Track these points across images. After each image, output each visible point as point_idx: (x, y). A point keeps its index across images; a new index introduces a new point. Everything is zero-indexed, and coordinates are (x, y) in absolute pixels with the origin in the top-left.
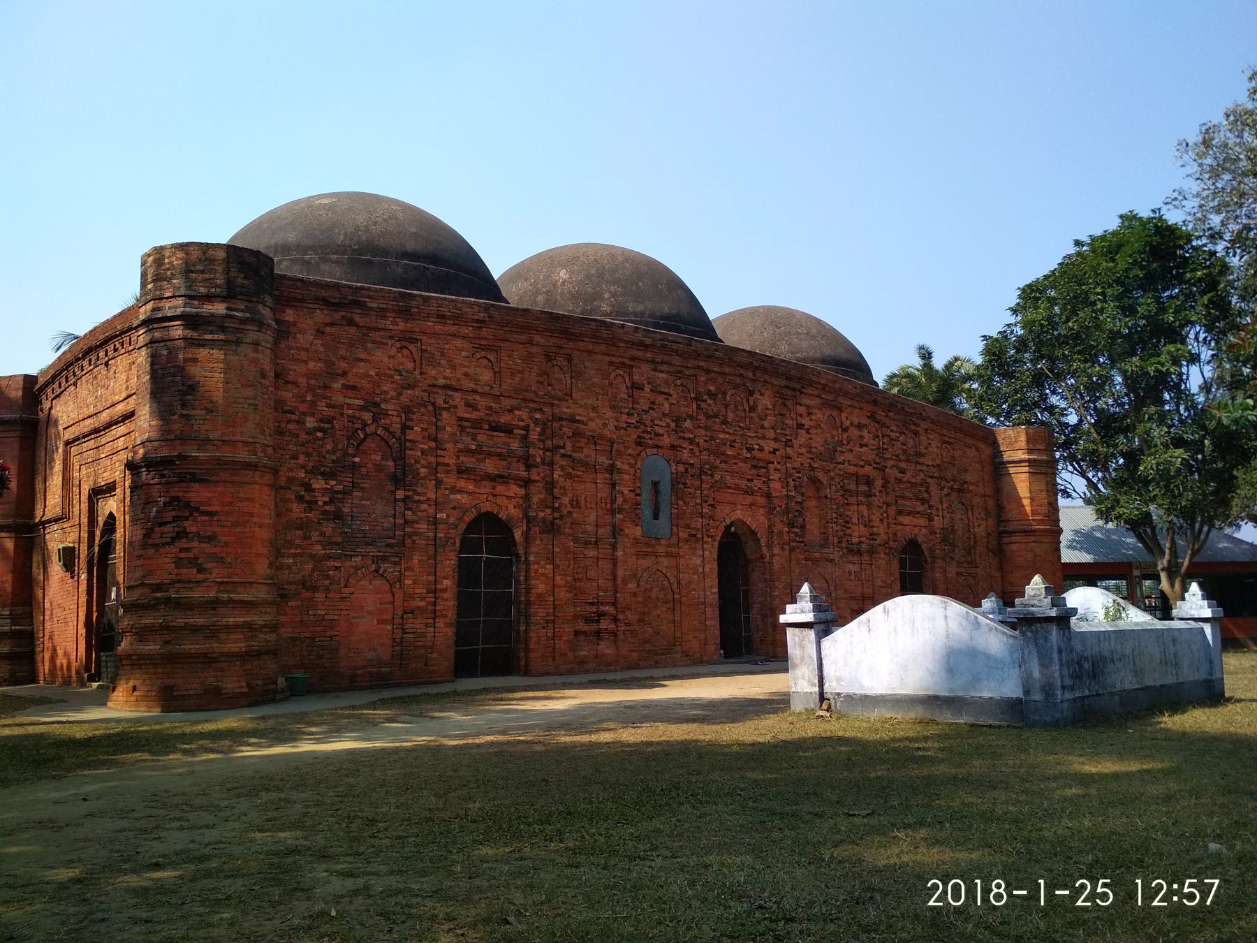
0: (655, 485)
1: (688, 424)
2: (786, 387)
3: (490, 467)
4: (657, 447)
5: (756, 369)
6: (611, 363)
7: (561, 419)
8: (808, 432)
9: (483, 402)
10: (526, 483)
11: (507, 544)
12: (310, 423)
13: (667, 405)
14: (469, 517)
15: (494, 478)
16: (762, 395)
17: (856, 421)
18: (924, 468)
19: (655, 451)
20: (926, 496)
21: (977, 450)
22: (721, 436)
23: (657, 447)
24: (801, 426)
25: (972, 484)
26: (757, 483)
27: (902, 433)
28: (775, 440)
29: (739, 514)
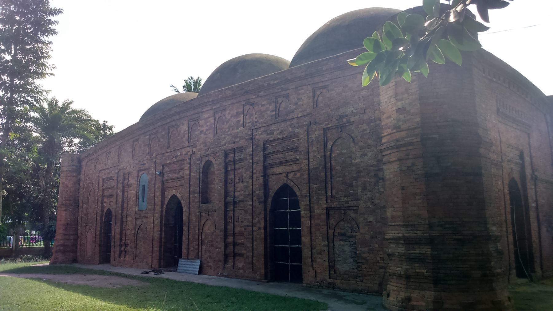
0: (144, 186)
2: (194, 114)
4: (145, 170)
6: (134, 141)
7: (120, 170)
8: (205, 134)
9: (108, 171)
17: (235, 112)
18: (295, 121)
19: (144, 172)
22: (167, 154)
23: (145, 170)
24: (202, 132)
25: (354, 114)
27: (270, 104)
28: (189, 146)
29: (173, 192)
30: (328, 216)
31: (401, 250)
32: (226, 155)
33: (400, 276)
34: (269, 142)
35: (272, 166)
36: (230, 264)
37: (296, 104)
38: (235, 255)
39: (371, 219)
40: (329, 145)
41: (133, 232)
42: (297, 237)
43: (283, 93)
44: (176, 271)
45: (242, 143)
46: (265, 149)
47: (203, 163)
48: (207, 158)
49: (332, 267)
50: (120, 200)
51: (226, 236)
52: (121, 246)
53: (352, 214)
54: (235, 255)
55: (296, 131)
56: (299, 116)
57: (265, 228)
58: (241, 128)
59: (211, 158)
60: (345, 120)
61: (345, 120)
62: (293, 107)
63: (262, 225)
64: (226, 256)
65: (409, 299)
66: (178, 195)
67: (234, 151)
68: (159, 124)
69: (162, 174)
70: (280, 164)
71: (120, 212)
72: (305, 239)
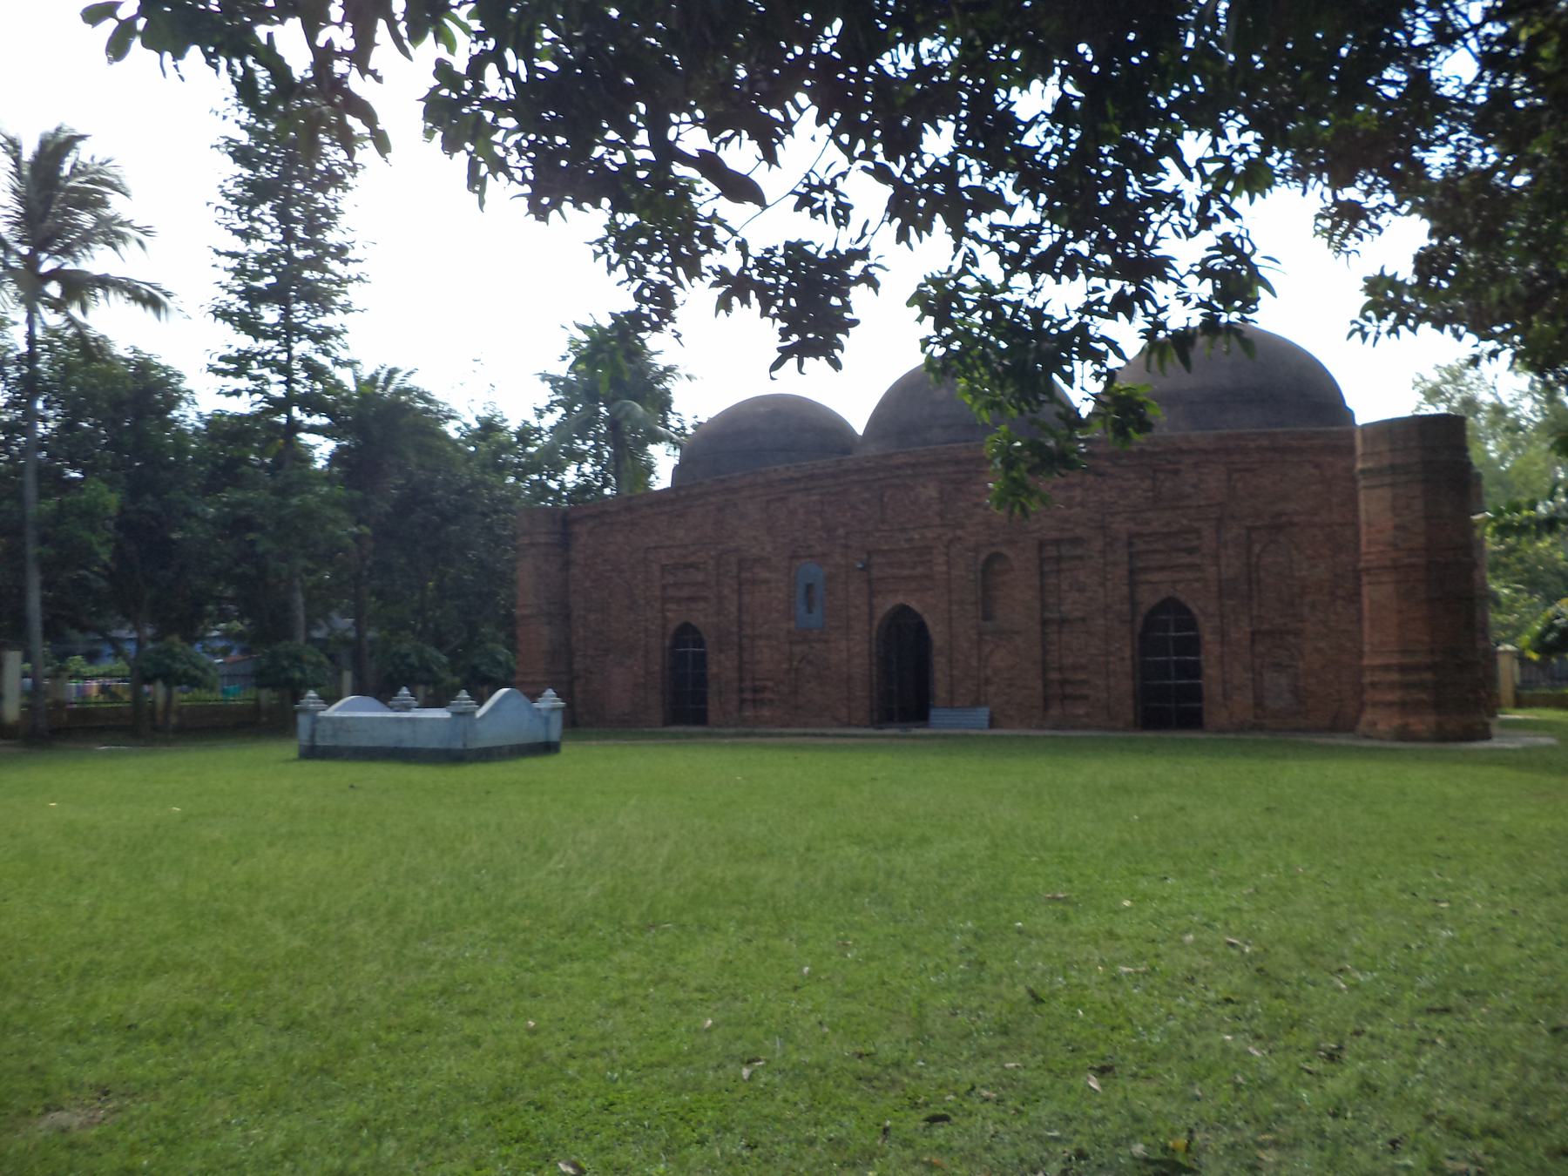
0: (809, 588)
1: (841, 531)
3: (686, 592)
5: (914, 466)
10: (705, 599)
11: (700, 643)
12: (588, 584)
13: (819, 522)
14: (672, 627)
15: (691, 599)
16: (925, 487)
20: (1196, 543)
21: (1317, 466)
23: (811, 556)
26: (920, 570)
28: (943, 526)
29: (901, 599)
30: (1253, 641)
31: (1395, 677)
32: (1042, 545)
33: (1390, 704)
34: (1139, 535)
35: (1146, 569)
36: (1055, 711)
37: (1194, 486)
38: (1064, 697)
39: (1322, 644)
40: (1257, 548)
41: (785, 666)
42: (1195, 670)
43: (1170, 467)
44: (926, 726)
45: (1079, 531)
46: (1130, 544)
47: (983, 557)
48: (994, 549)
49: (1259, 704)
50: (733, 609)
51: (1045, 671)
52: (741, 691)
53: (1291, 639)
54: (1064, 697)
55: (1196, 525)
56: (1202, 503)
57: (1132, 657)
58: (1078, 509)
59: (1004, 550)
60: (1284, 519)
61: (1284, 519)
62: (1189, 490)
63: (1127, 653)
64: (1046, 699)
65: (1406, 725)
66: (914, 605)
67: (1057, 542)
68: (855, 478)
69: (867, 567)
70: (1161, 569)
71: (735, 629)
72: (1211, 671)
